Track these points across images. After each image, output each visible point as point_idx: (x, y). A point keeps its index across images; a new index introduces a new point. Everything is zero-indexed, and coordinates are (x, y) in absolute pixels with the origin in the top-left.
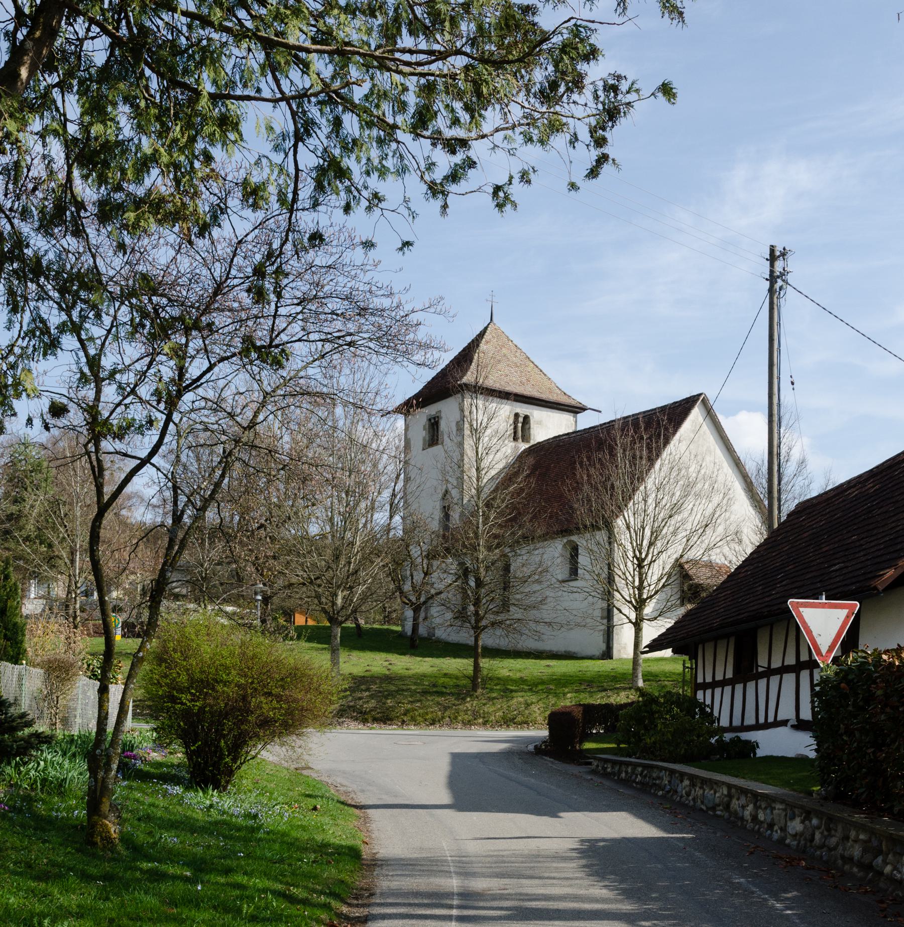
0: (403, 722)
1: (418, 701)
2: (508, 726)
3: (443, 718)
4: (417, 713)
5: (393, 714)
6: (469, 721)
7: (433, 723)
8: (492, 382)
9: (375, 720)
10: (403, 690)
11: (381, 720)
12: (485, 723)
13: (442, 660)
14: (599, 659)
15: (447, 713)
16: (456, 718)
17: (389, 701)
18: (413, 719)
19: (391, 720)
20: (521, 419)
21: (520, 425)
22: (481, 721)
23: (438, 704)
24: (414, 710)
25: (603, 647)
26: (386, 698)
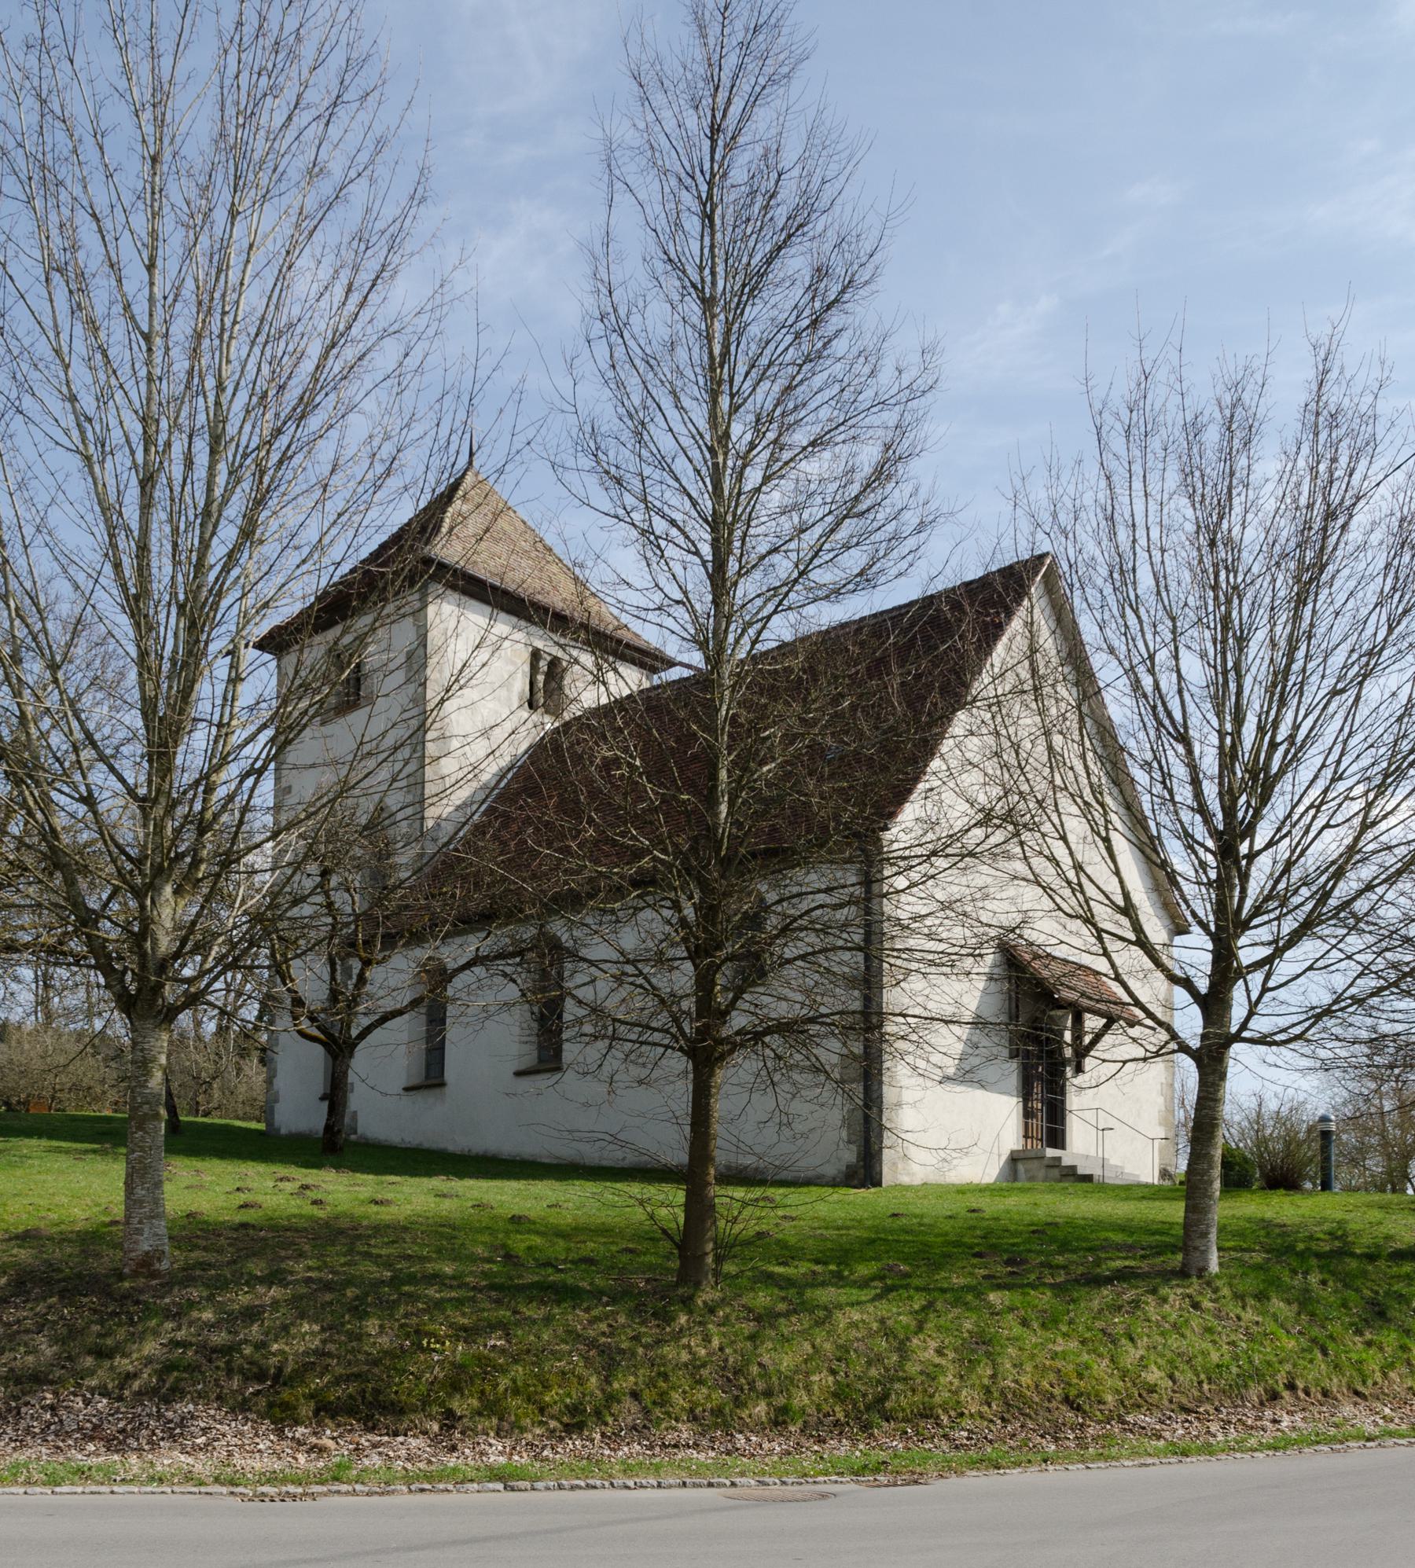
0: (450, 1420)
1: (493, 1327)
2: (866, 1427)
3: (611, 1398)
4: (504, 1382)
5: (403, 1388)
6: (718, 1412)
7: (575, 1422)
8: (486, 565)
9: (326, 1410)
10: (412, 1279)
11: (352, 1412)
12: (779, 1420)
13: (470, 1183)
14: (834, 1184)
15: (623, 1383)
16: (663, 1400)
17: (372, 1326)
18: (491, 1407)
19: (398, 1410)
20: (543, 665)
21: (541, 678)
22: (761, 1409)
23: (573, 1336)
24: (487, 1367)
25: (850, 1155)
26: (359, 1311)
